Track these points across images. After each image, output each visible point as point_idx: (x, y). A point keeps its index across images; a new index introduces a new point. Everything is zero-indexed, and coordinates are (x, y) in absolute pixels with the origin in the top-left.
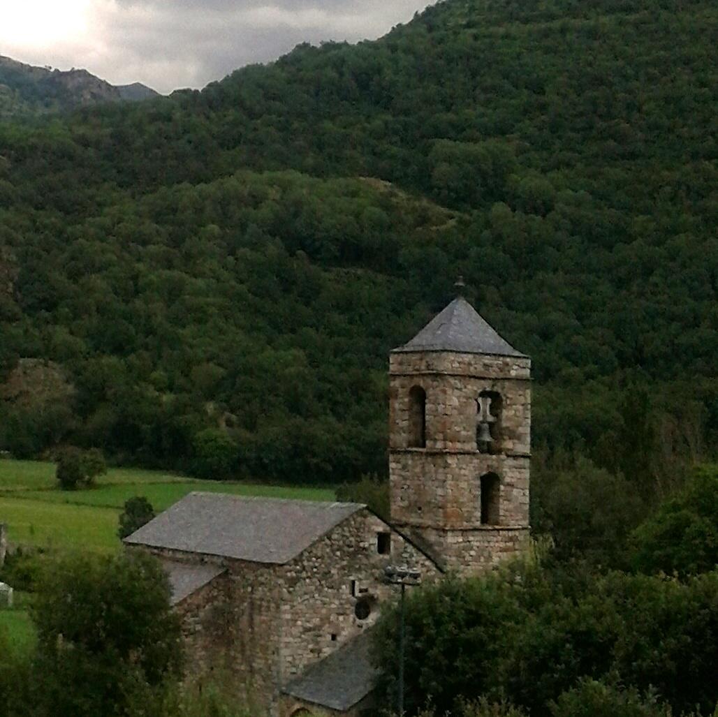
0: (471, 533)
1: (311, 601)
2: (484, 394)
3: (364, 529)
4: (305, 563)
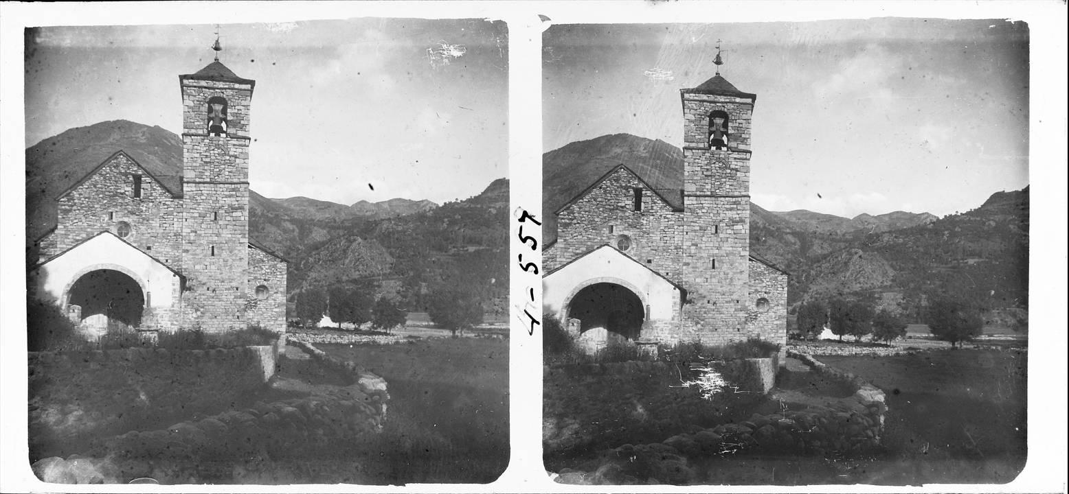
1: (579, 237)
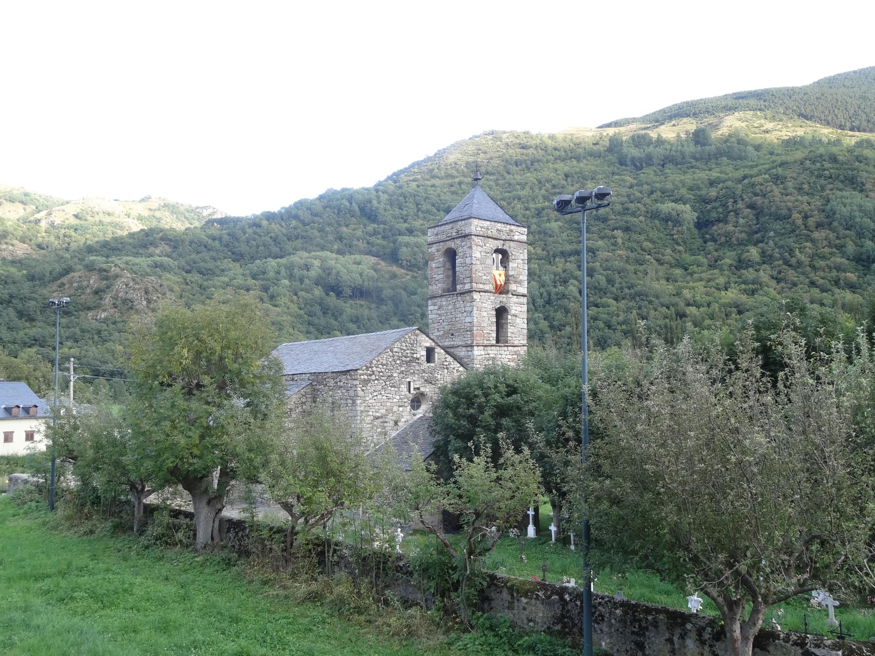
1: (379, 397)
2: (497, 251)
4: (374, 369)
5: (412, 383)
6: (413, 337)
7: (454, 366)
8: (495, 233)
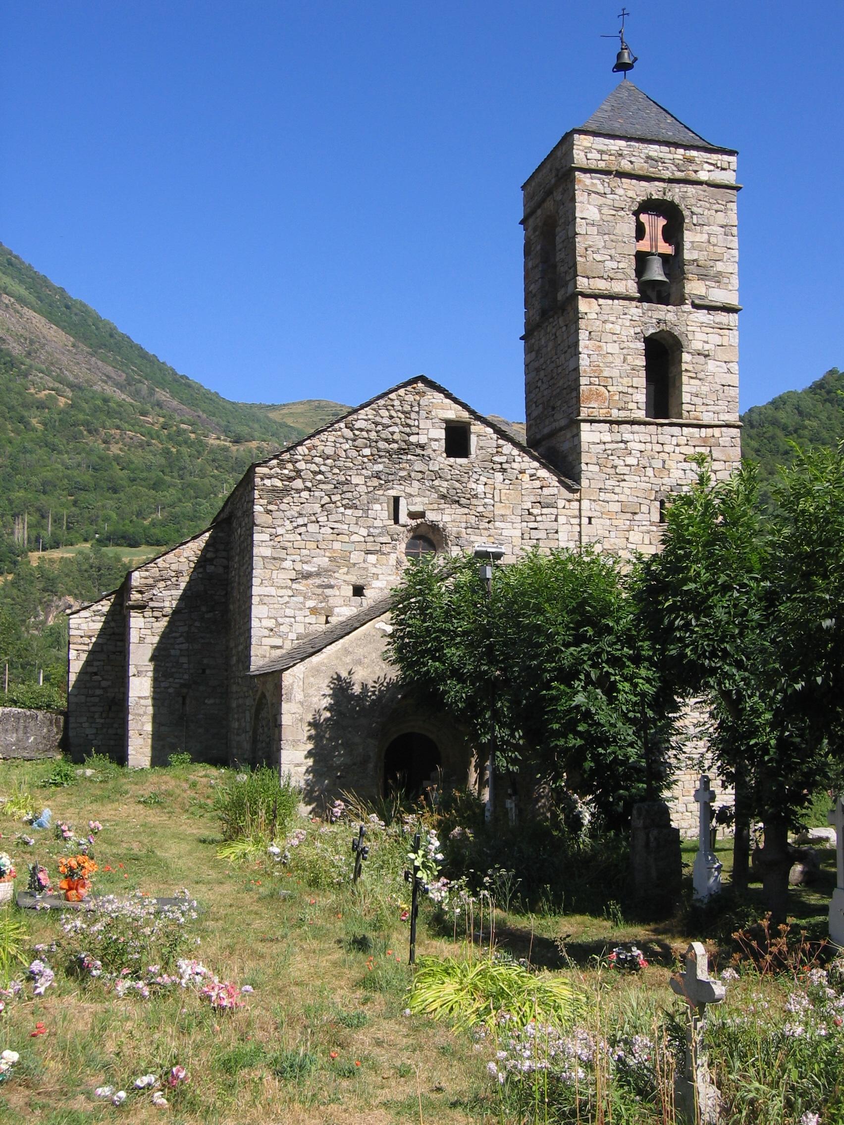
0: (628, 426)
1: (313, 528)
2: (649, 206)
3: (418, 412)
4: (301, 465)
5: (403, 502)
6: (410, 398)
7: (524, 466)
8: (640, 166)
